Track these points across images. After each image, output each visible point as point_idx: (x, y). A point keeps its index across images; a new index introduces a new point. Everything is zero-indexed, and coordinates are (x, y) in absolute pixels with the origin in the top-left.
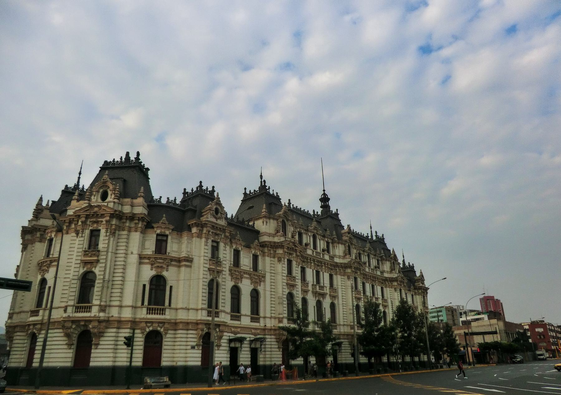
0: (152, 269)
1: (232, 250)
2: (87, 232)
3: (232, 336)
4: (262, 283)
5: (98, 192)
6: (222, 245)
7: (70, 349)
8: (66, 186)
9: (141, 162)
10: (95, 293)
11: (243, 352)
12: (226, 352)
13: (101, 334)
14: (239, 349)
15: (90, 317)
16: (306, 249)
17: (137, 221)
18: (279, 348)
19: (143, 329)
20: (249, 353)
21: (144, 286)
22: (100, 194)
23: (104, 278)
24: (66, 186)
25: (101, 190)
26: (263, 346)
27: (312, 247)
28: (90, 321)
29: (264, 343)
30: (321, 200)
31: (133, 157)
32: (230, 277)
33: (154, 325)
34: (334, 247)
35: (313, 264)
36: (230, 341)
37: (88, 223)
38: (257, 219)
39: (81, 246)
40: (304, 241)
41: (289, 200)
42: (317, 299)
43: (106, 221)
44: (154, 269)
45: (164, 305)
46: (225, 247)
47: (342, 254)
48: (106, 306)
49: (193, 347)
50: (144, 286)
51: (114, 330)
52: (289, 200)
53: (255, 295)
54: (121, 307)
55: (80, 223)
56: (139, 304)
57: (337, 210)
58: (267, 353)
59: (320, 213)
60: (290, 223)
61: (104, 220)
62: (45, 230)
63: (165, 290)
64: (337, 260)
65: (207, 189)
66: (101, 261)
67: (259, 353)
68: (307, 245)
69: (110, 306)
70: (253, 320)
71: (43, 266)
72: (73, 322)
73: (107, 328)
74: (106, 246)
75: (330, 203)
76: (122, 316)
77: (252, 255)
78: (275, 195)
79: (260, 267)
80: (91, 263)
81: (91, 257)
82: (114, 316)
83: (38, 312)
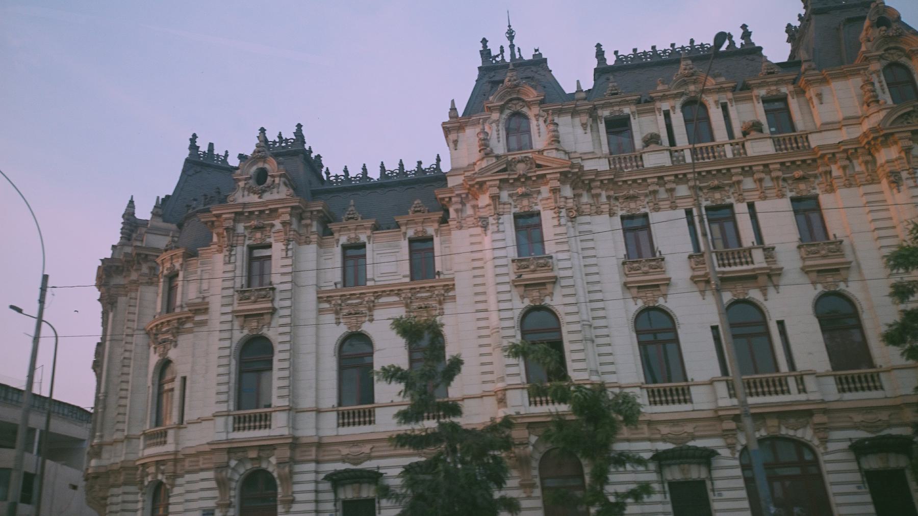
10: (276, 383)
81: (255, 302)
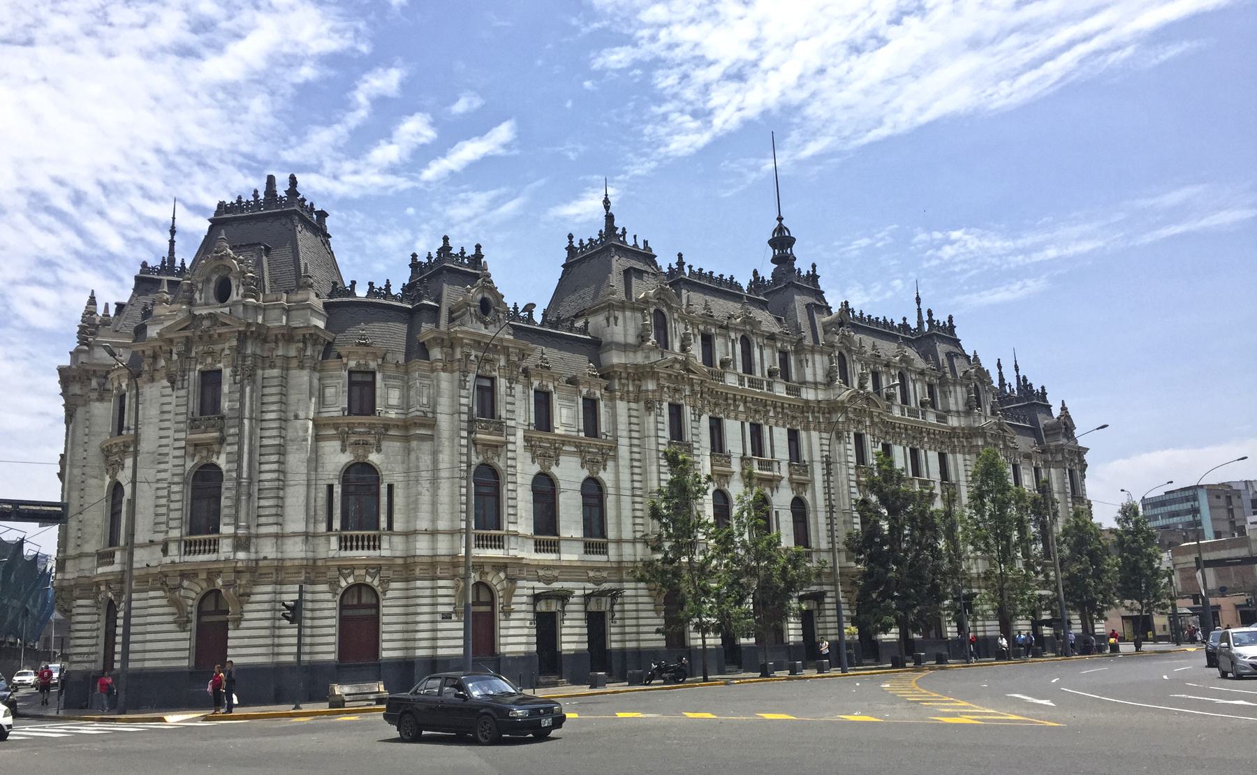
0: (343, 450)
1: (532, 393)
2: (194, 376)
3: (540, 587)
4: (610, 464)
5: (208, 280)
6: (502, 384)
7: (184, 631)
8: (144, 265)
9: (304, 200)
10: (224, 511)
11: (567, 623)
12: (528, 623)
13: (245, 597)
14: (559, 616)
15: (217, 561)
16: (721, 376)
17: (301, 345)
18: (655, 610)
19: (334, 584)
20: (583, 623)
21: (330, 488)
22: (212, 285)
23: (239, 476)
24: (144, 265)
25: (215, 278)
26: (616, 607)
27: (740, 370)
28: (219, 573)
29: (619, 600)
30: (772, 243)
31: (281, 191)
32: (529, 455)
33: (357, 572)
34: (800, 363)
35: (741, 408)
36: (536, 598)
37: (193, 354)
38: (595, 312)
39: (183, 409)
40: (718, 356)
41: (680, 255)
43: (230, 348)
45: (377, 528)
46: (510, 388)
47: (820, 377)
48: (248, 538)
49: (446, 617)
50: (330, 488)
51: (269, 588)
52: (680, 255)
53: (593, 493)
54: (279, 537)
55: (175, 357)
56: (322, 528)
57: (814, 266)
58: (628, 622)
59: (768, 277)
60: (676, 316)
61: (227, 345)
62: (108, 373)
63: (377, 494)
64: (809, 395)
65: (463, 252)
66: (230, 439)
67: (609, 622)
68: (724, 363)
69: (258, 536)
70: (589, 548)
71: (111, 458)
72: (183, 575)
73: (256, 584)
74: (238, 405)
75: (796, 250)
76: (286, 556)
77: (580, 401)
78: (641, 246)
79: (604, 426)
80: (207, 446)
82: (270, 557)
83: (112, 555)
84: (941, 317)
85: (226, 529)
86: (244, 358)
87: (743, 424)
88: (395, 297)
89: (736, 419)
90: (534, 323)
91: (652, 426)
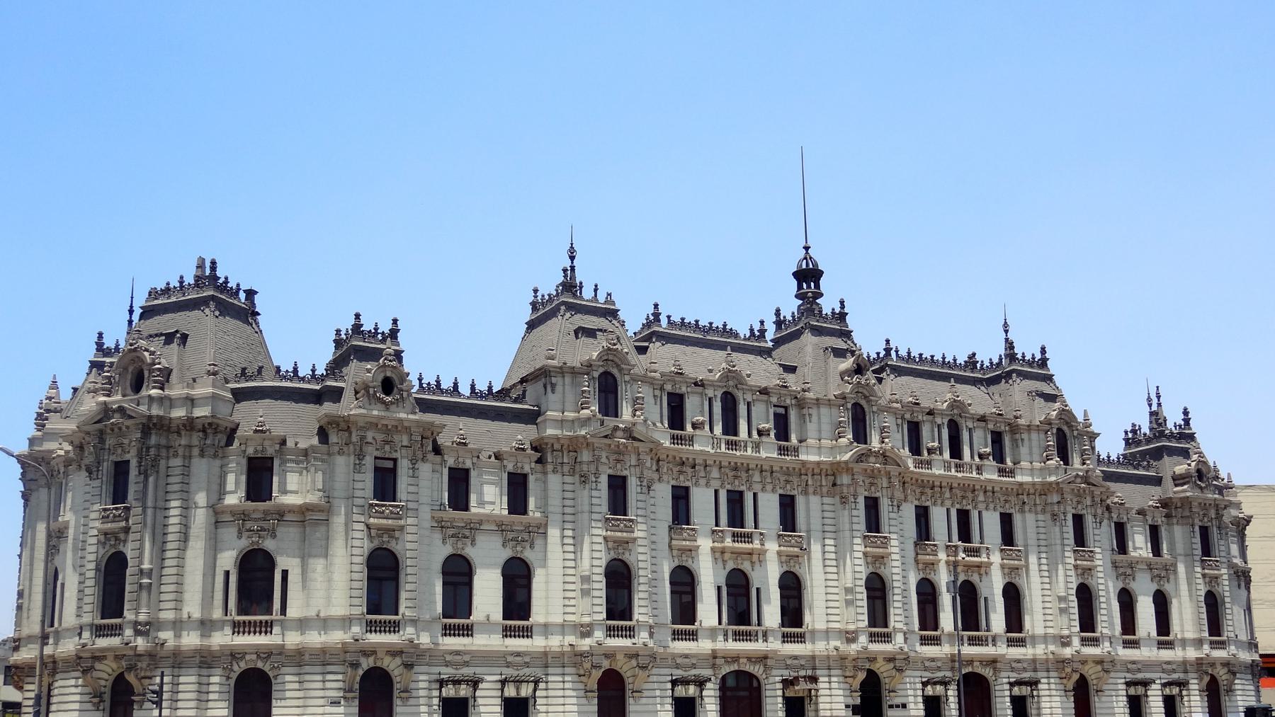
0: (240, 537)
4: (539, 542)
6: (404, 466)
21: (227, 573)
25: (131, 369)
26: (538, 693)
33: (248, 657)
34: (802, 418)
41: (656, 306)
42: (731, 565)
44: (245, 534)
50: (227, 573)
56: (217, 614)
66: (134, 528)
84: (1027, 348)
85: (129, 615)
86: (148, 448)
87: (716, 492)
88: (303, 379)
89: (707, 485)
90: (459, 395)
91: (586, 501)
